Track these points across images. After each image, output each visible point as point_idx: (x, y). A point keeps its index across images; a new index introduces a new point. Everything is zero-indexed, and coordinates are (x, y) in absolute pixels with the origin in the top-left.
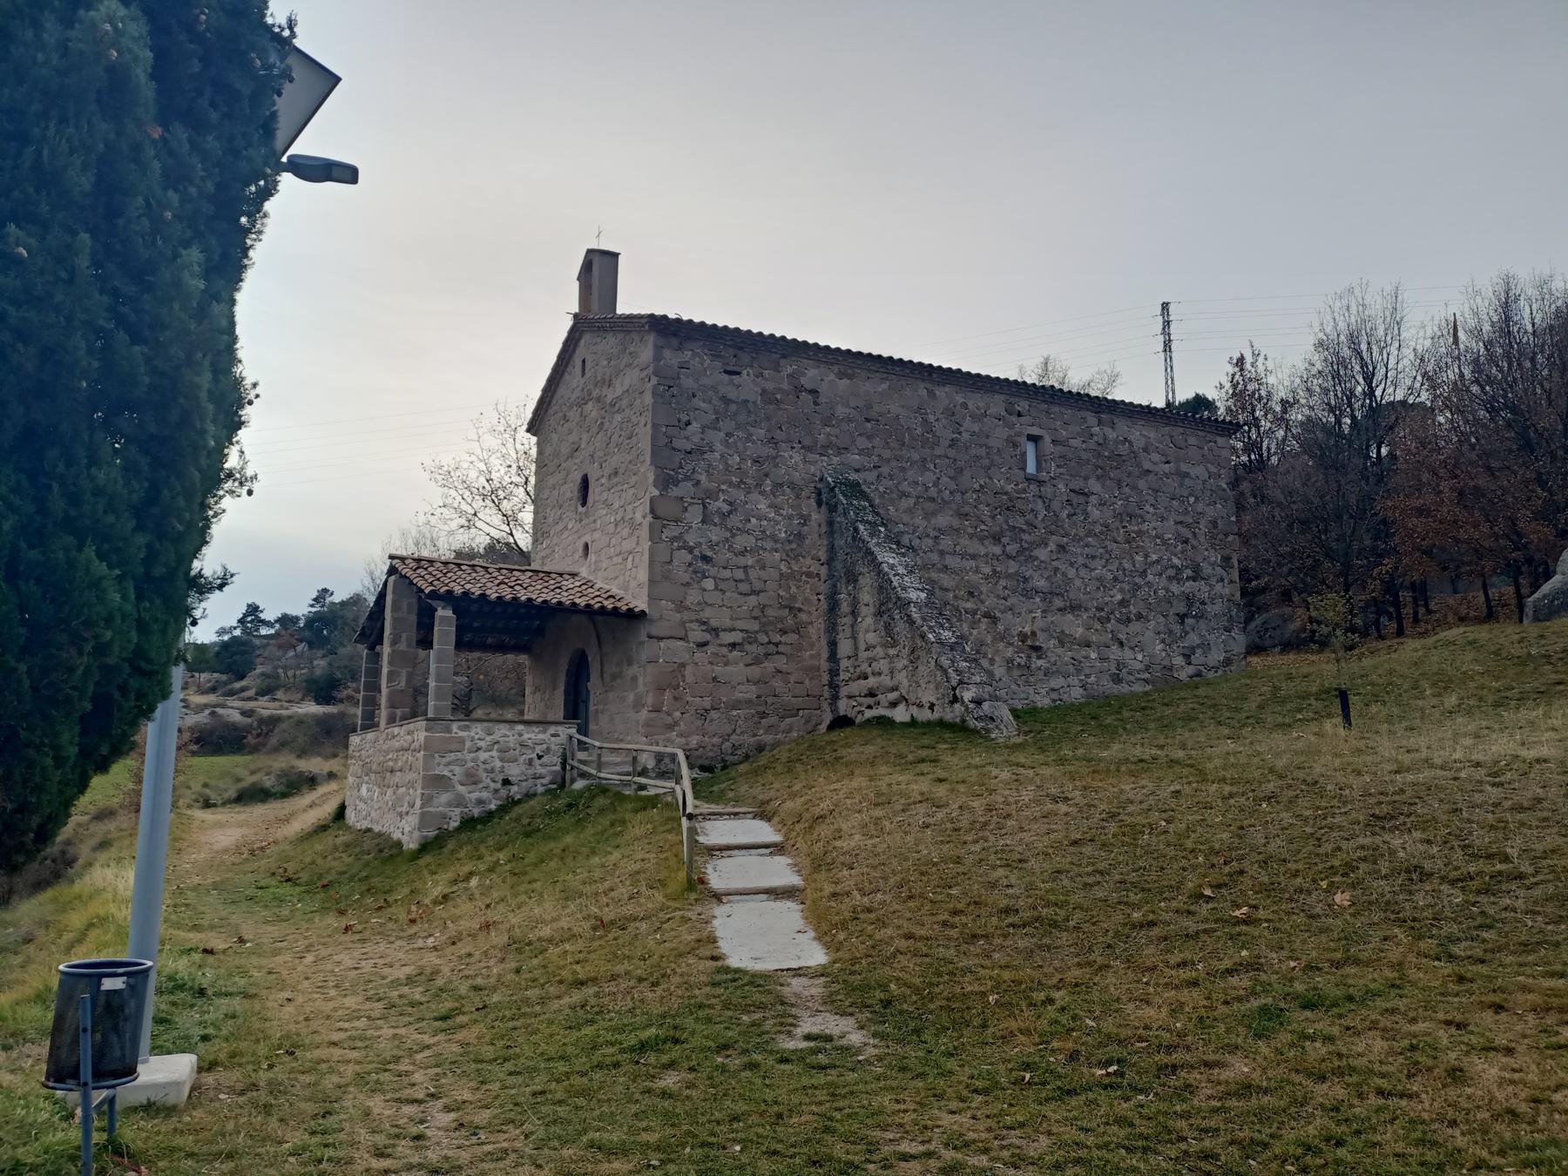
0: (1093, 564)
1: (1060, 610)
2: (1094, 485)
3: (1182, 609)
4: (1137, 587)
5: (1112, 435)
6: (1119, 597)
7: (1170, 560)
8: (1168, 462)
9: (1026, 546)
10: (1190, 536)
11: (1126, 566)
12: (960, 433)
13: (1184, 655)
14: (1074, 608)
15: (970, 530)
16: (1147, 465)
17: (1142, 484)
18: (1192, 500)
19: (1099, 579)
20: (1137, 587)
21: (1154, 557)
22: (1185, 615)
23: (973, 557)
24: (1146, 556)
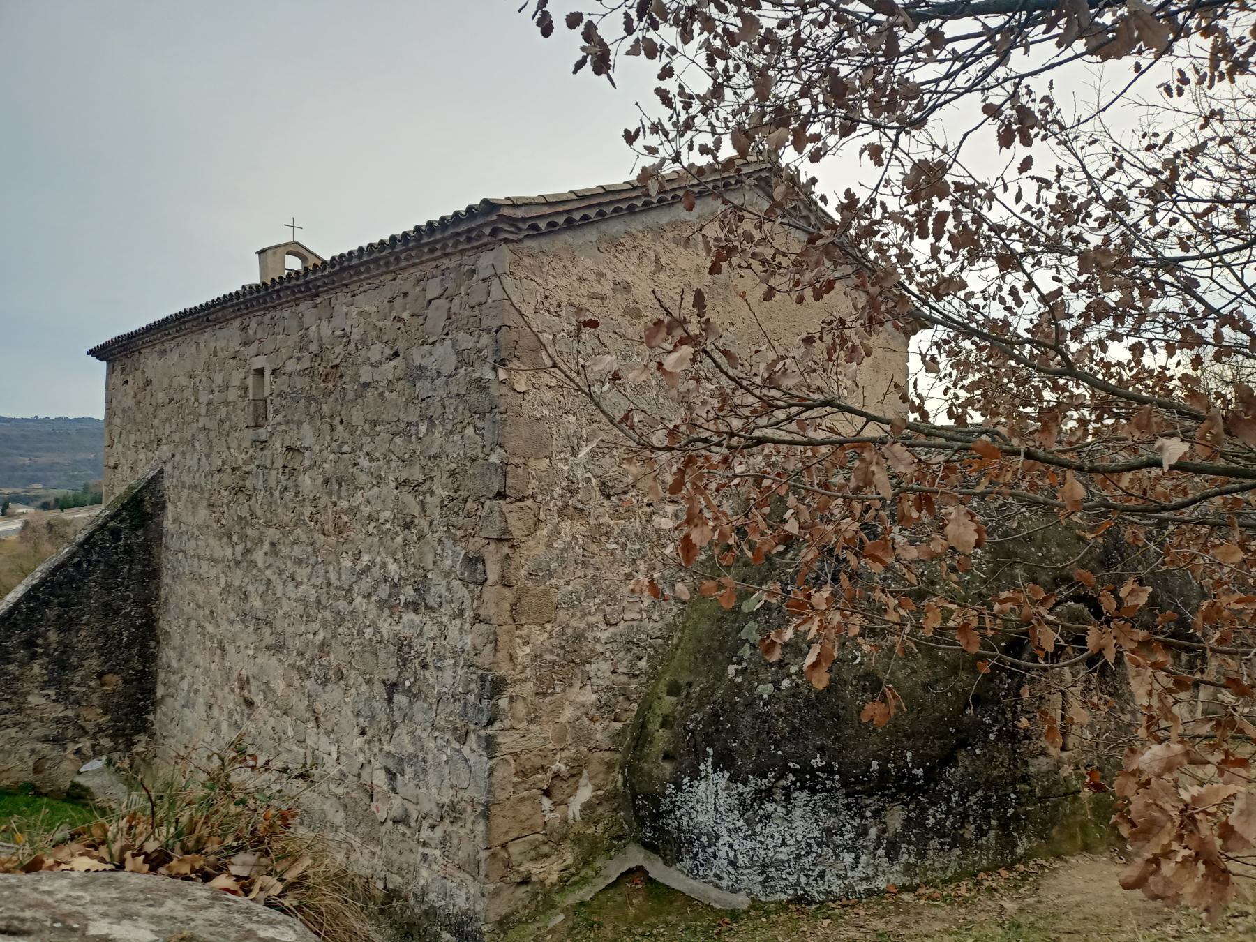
0: (302, 573)
1: (268, 648)
2: (307, 436)
3: (393, 675)
4: (339, 619)
5: (326, 329)
6: (321, 636)
7: (384, 565)
8: (396, 354)
9: (249, 544)
10: (416, 511)
11: (333, 577)
12: (212, 392)
13: (388, 771)
14: (278, 648)
15: (215, 526)
16: (365, 374)
17: (356, 416)
18: (423, 428)
19: (303, 600)
20: (339, 619)
21: (366, 558)
22: (394, 685)
23: (216, 561)
24: (357, 557)
